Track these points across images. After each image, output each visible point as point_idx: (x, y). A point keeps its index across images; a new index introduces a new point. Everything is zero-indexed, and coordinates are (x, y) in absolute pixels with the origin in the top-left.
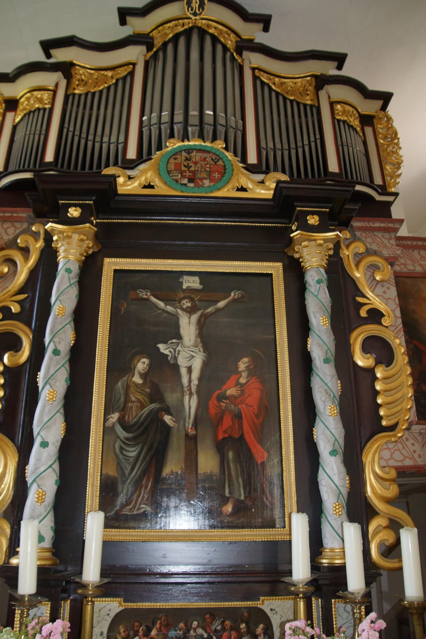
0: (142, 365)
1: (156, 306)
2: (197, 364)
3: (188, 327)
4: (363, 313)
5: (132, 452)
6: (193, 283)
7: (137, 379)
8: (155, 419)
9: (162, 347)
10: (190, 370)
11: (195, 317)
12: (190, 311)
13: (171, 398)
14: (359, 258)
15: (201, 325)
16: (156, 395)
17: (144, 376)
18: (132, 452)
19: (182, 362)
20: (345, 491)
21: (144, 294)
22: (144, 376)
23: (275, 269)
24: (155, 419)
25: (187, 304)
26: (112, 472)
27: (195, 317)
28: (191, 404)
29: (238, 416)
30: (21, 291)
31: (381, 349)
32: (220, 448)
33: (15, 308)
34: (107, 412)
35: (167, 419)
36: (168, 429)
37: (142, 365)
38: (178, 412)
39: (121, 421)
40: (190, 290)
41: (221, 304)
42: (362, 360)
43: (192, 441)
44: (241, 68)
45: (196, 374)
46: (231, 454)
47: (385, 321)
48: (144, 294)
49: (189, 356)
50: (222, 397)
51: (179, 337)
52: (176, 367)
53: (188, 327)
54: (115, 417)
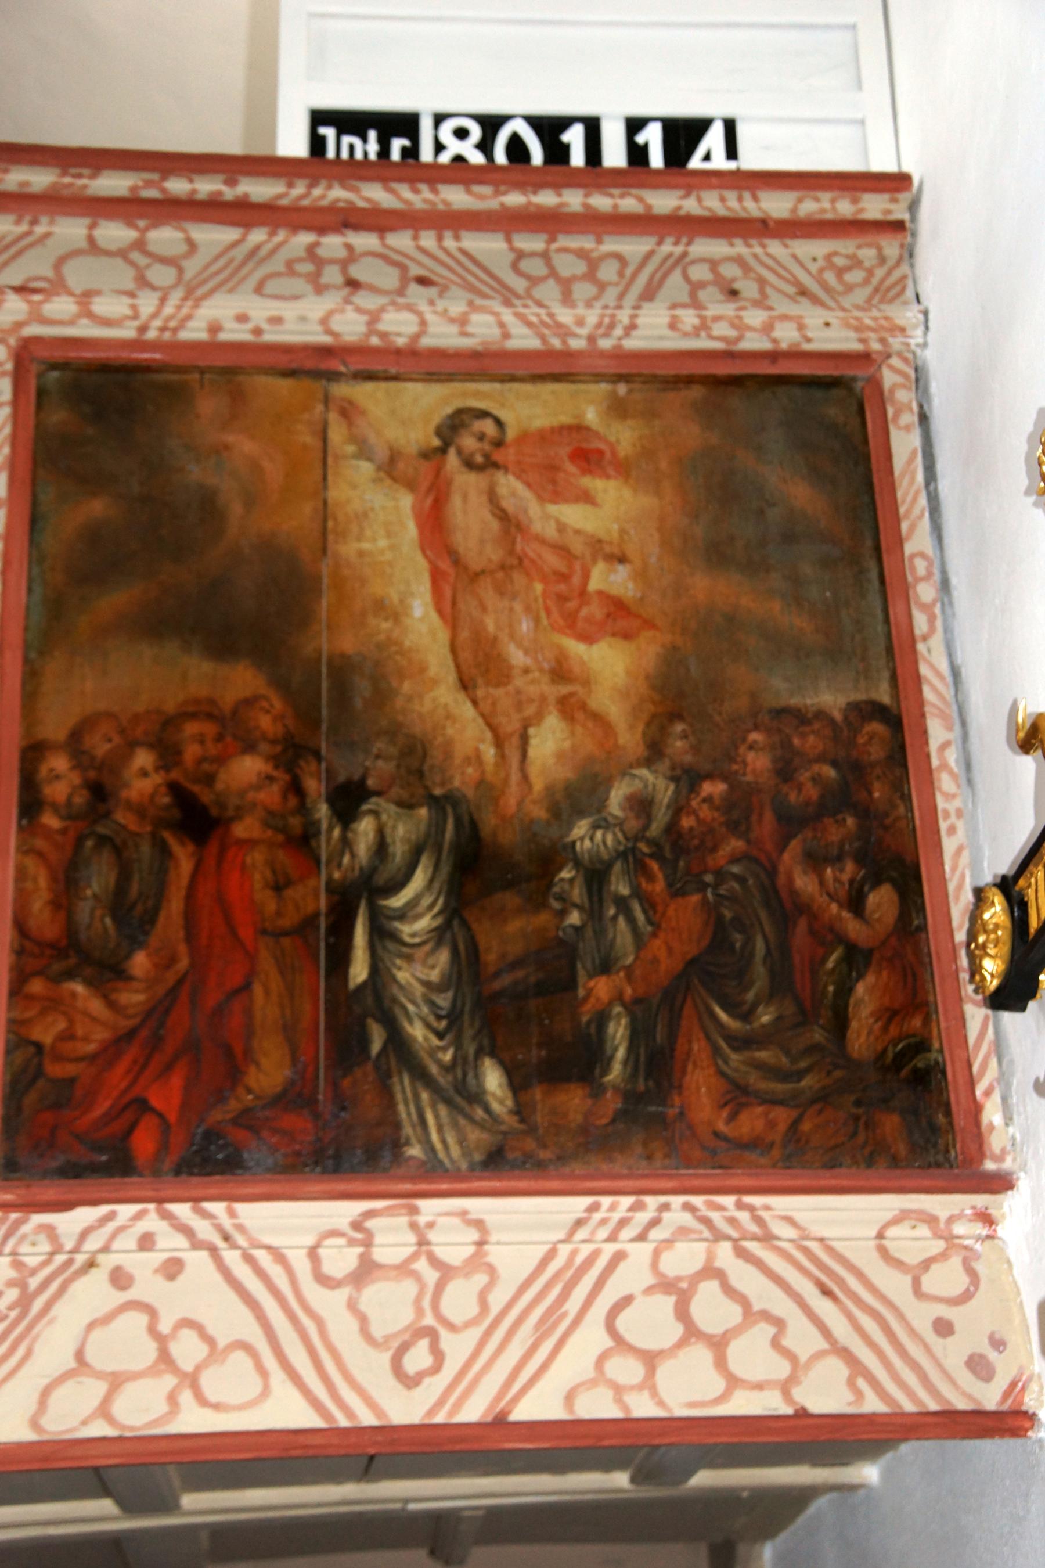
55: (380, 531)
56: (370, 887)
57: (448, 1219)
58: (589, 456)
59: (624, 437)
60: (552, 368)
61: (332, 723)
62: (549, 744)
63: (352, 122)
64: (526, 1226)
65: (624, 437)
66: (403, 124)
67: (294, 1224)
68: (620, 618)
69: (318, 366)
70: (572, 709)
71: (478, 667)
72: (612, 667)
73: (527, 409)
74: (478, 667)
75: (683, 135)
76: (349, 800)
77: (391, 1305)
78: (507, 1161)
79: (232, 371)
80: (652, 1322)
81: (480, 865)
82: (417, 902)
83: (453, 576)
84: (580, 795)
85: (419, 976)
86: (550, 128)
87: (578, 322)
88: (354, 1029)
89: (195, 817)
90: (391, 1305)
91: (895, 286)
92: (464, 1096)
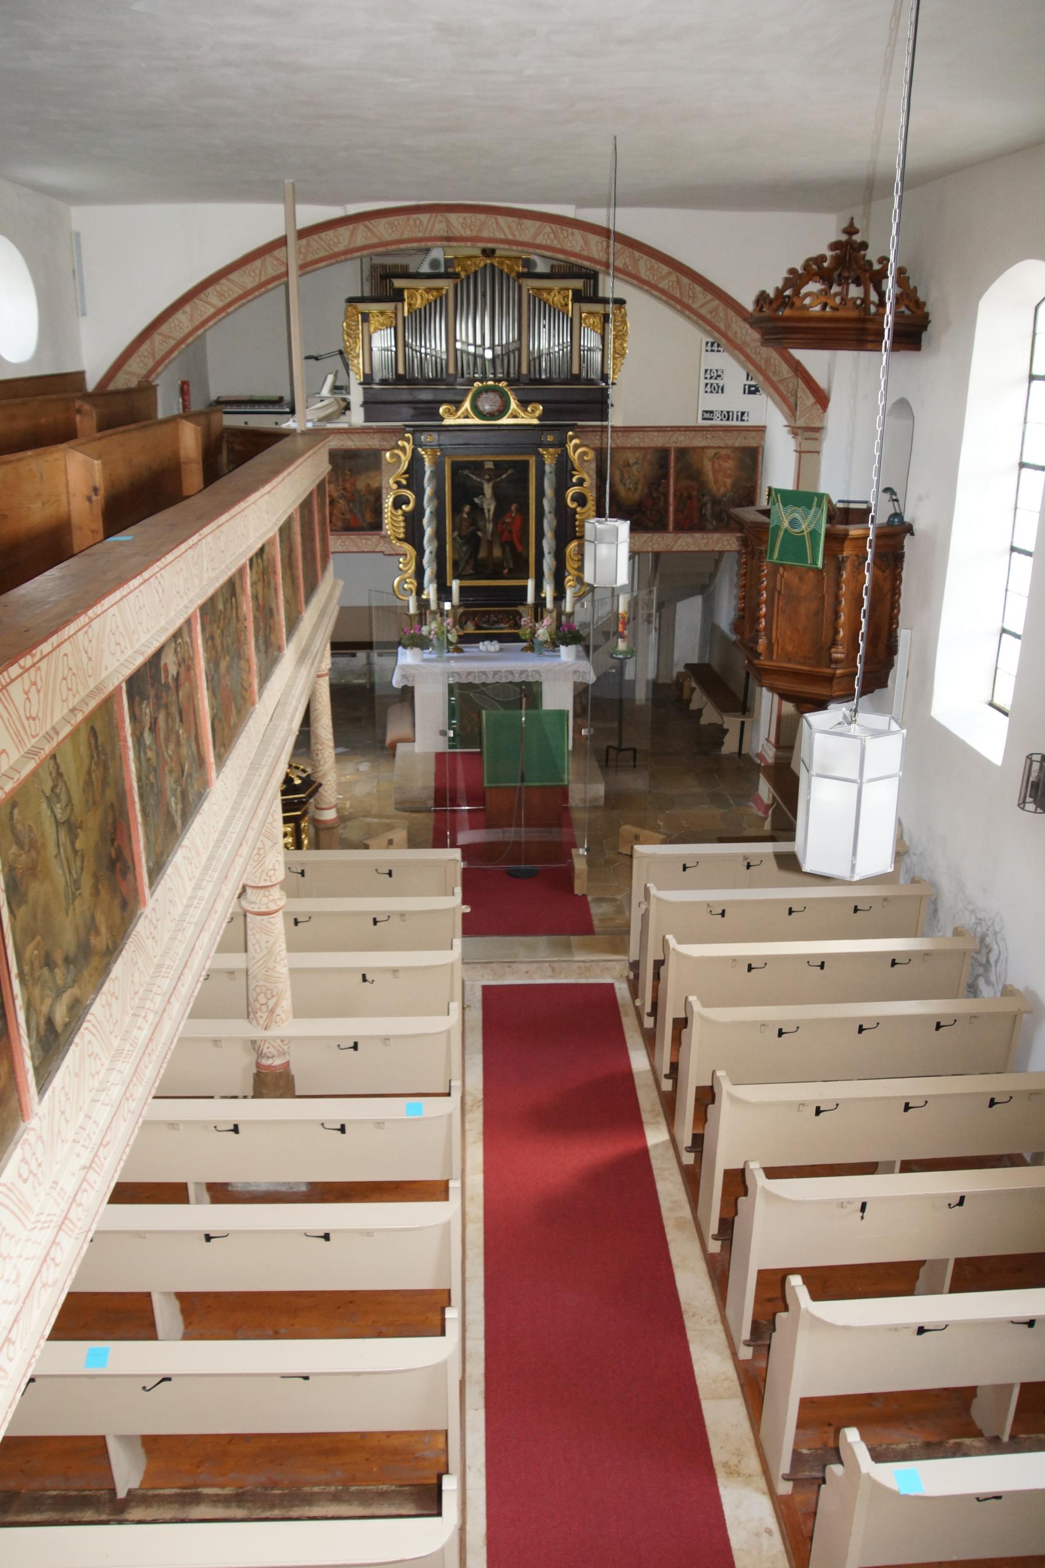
0: (467, 508)
1: (472, 479)
2: (492, 507)
3: (488, 489)
4: (574, 480)
5: (464, 549)
6: (489, 465)
7: (465, 516)
8: (473, 534)
9: (476, 500)
10: (489, 510)
11: (491, 484)
12: (489, 481)
13: (481, 523)
14: (576, 447)
15: (494, 488)
16: (473, 522)
17: (468, 514)
18: (464, 549)
19: (485, 507)
20: (553, 568)
21: (466, 472)
22: (468, 514)
23: (533, 461)
24: (473, 534)
25: (487, 477)
26: (457, 557)
27: (491, 484)
28: (490, 527)
29: (511, 532)
30: (405, 473)
31: (581, 500)
32: (503, 546)
33: (404, 482)
34: (453, 530)
35: (479, 533)
36: (479, 538)
37: (467, 508)
38: (485, 532)
39: (459, 535)
40: (489, 469)
41: (504, 476)
42: (571, 505)
43: (490, 543)
44: (520, 287)
45: (492, 512)
46: (507, 549)
47: (585, 484)
48: (466, 472)
49: (489, 504)
50: (504, 523)
51: (483, 494)
52: (482, 509)
53: (488, 489)
54: (456, 533)
55: (708, 467)
56: (705, 504)
57: (710, 535)
58: (729, 458)
59: (732, 455)
60: (726, 447)
61: (702, 487)
62: (722, 489)
63: (707, 412)
64: (716, 536)
65: (732, 455)
66: (712, 412)
67: (698, 535)
68: (730, 476)
69: (703, 448)
70: (725, 486)
71: (716, 482)
72: (729, 481)
73: (723, 452)
74: (716, 482)
75: (743, 414)
76: (703, 495)
77: (705, 541)
78: (715, 530)
79: (694, 448)
80: (726, 543)
81: (715, 502)
82: (709, 506)
83: (714, 471)
84: (724, 495)
85: (709, 512)
86: (728, 412)
87: (730, 443)
88: (702, 516)
89: (690, 497)
90: (705, 541)
91: (762, 438)
92: (712, 523)
